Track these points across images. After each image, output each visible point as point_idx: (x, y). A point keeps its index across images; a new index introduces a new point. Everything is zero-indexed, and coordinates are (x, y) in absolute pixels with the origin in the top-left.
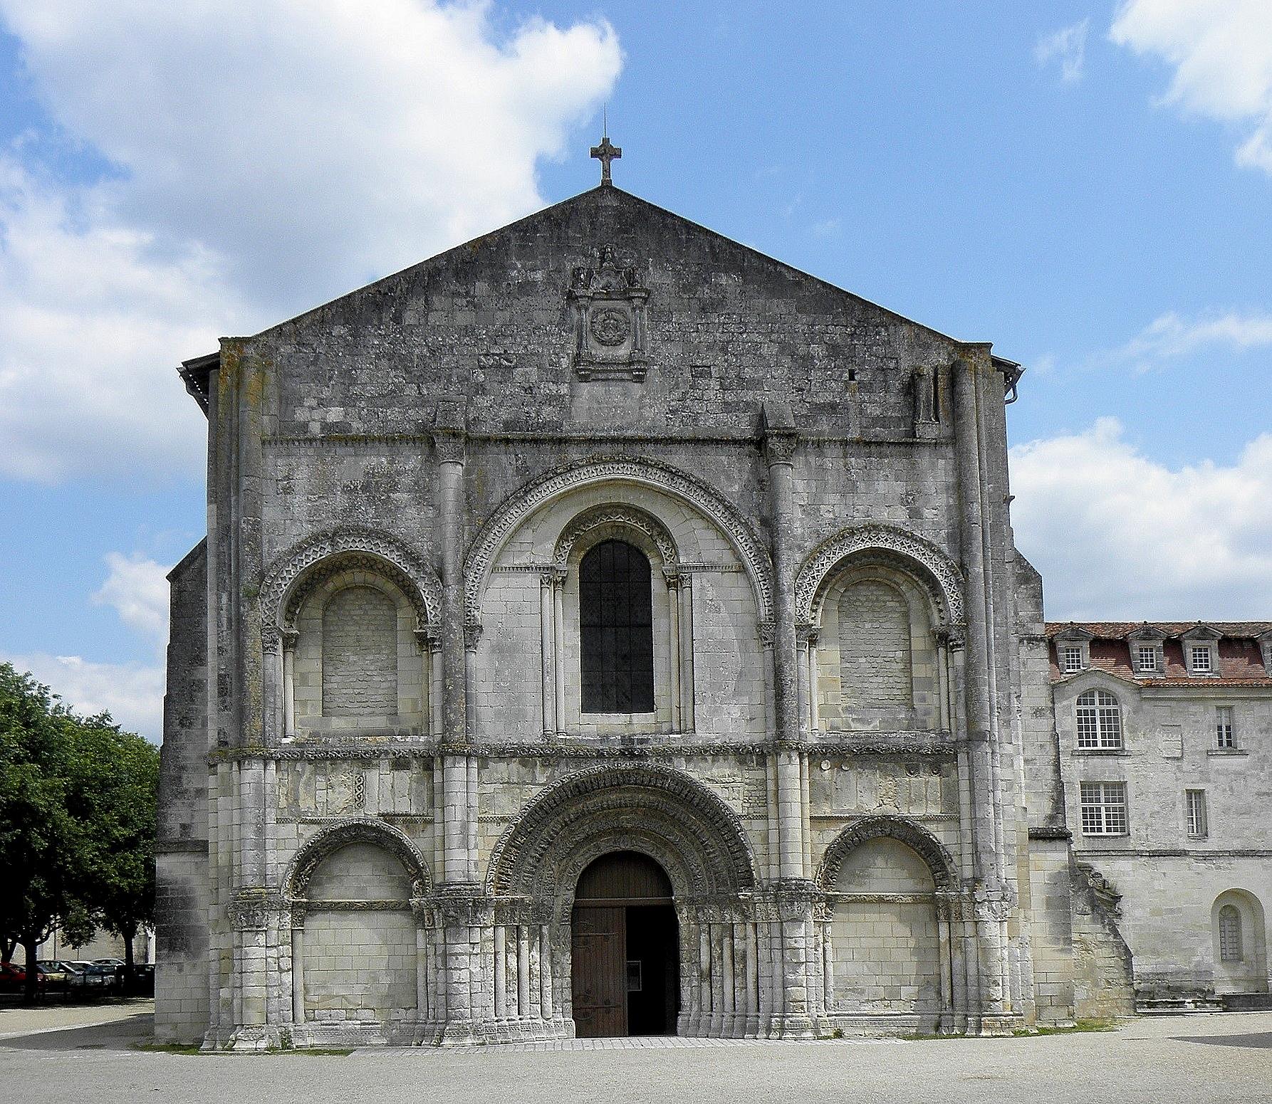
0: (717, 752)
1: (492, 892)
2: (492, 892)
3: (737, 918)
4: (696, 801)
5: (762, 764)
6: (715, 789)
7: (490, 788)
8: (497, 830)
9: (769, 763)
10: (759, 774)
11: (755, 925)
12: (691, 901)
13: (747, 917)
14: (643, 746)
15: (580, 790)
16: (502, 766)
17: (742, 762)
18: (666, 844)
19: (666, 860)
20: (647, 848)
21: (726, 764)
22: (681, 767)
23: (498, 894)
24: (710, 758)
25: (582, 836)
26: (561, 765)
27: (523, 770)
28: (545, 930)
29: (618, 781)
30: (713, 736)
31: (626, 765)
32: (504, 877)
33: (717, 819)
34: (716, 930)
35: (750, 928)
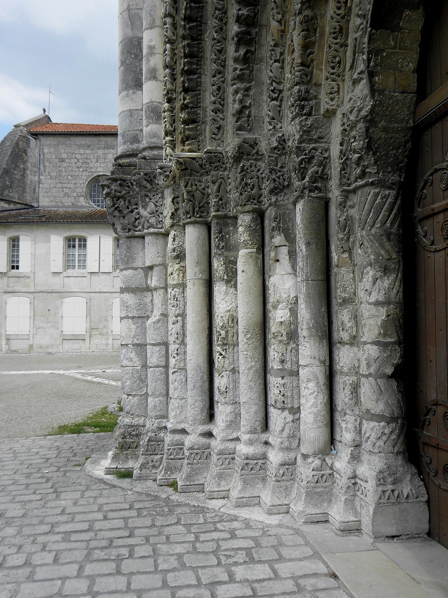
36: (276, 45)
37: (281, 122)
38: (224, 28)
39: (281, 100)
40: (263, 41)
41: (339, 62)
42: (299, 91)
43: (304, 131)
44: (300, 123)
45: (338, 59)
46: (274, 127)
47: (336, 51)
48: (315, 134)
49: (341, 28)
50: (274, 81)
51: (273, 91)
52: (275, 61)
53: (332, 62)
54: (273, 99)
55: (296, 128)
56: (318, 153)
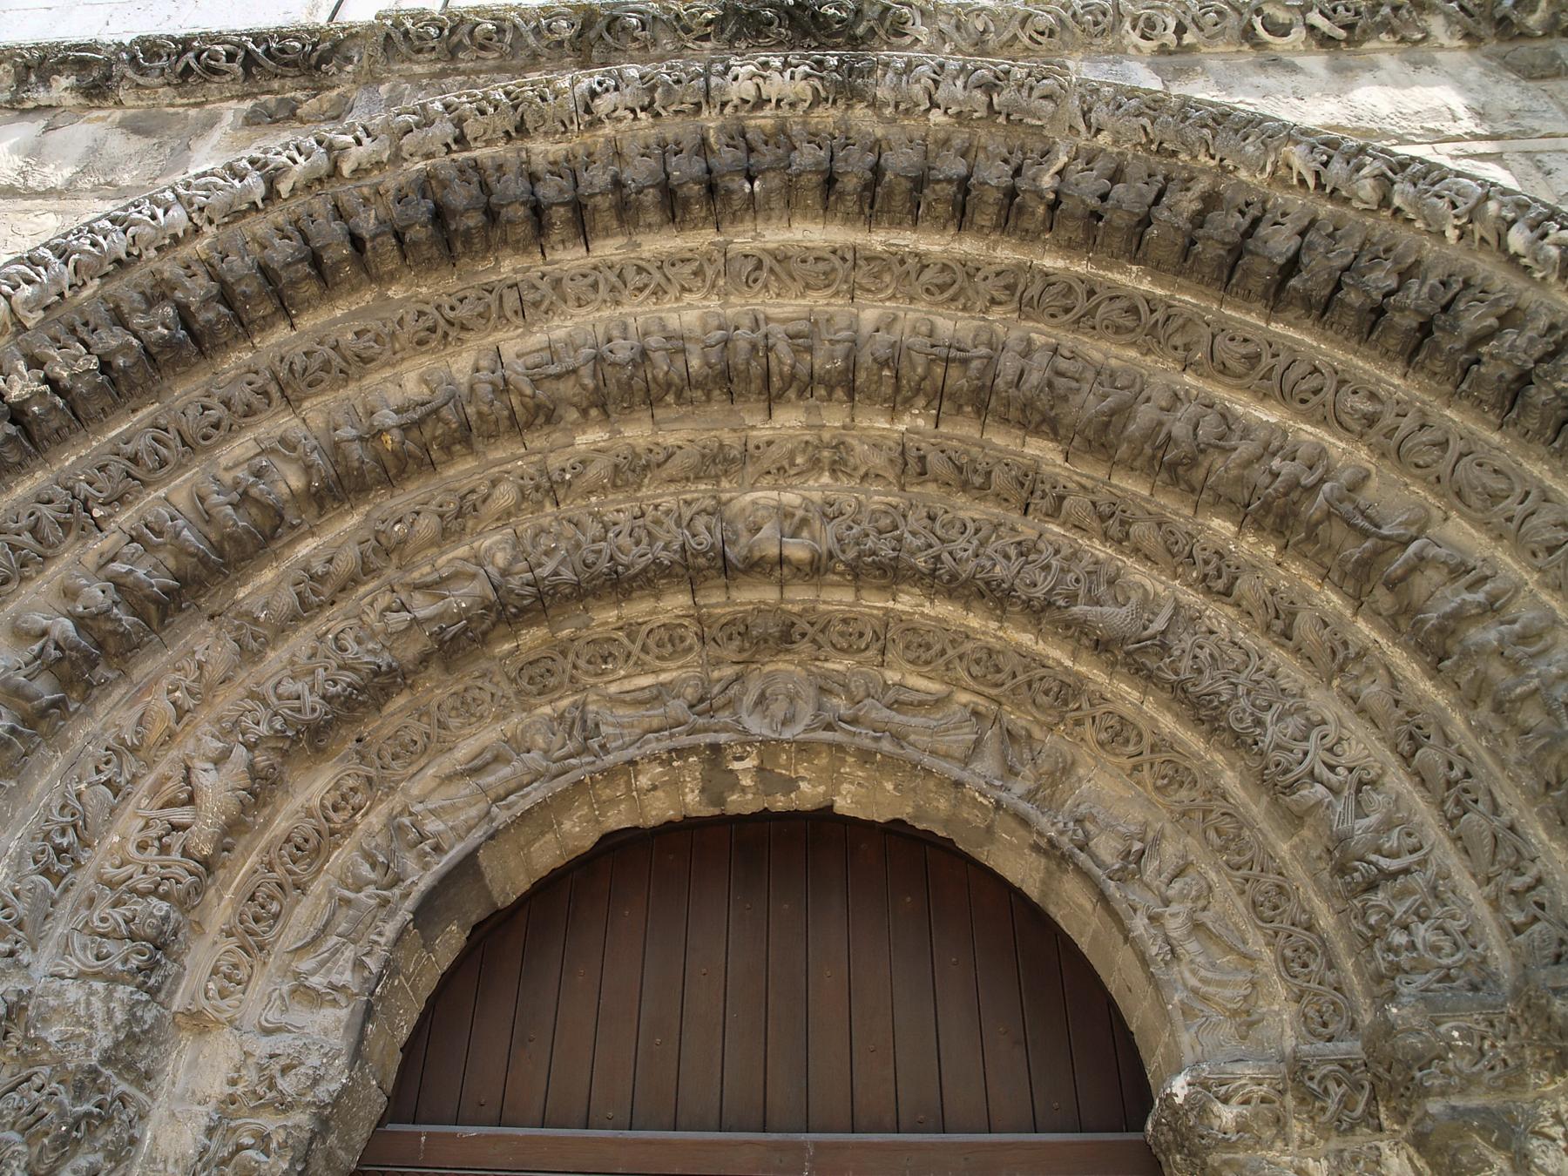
25: (461, 597)
36: (133, 750)
37: (34, 950)
38: (12, 586)
39: (66, 890)
40: (101, 709)
41: (276, 916)
42: (165, 919)
43: (131, 1036)
44: (132, 1007)
45: (275, 907)
46: (11, 954)
47: (280, 886)
48: (145, 1057)
49: (317, 850)
50: (75, 826)
51: (59, 851)
52: (107, 783)
53: (263, 907)
54: (46, 872)
55: (110, 1014)
56: (124, 1117)
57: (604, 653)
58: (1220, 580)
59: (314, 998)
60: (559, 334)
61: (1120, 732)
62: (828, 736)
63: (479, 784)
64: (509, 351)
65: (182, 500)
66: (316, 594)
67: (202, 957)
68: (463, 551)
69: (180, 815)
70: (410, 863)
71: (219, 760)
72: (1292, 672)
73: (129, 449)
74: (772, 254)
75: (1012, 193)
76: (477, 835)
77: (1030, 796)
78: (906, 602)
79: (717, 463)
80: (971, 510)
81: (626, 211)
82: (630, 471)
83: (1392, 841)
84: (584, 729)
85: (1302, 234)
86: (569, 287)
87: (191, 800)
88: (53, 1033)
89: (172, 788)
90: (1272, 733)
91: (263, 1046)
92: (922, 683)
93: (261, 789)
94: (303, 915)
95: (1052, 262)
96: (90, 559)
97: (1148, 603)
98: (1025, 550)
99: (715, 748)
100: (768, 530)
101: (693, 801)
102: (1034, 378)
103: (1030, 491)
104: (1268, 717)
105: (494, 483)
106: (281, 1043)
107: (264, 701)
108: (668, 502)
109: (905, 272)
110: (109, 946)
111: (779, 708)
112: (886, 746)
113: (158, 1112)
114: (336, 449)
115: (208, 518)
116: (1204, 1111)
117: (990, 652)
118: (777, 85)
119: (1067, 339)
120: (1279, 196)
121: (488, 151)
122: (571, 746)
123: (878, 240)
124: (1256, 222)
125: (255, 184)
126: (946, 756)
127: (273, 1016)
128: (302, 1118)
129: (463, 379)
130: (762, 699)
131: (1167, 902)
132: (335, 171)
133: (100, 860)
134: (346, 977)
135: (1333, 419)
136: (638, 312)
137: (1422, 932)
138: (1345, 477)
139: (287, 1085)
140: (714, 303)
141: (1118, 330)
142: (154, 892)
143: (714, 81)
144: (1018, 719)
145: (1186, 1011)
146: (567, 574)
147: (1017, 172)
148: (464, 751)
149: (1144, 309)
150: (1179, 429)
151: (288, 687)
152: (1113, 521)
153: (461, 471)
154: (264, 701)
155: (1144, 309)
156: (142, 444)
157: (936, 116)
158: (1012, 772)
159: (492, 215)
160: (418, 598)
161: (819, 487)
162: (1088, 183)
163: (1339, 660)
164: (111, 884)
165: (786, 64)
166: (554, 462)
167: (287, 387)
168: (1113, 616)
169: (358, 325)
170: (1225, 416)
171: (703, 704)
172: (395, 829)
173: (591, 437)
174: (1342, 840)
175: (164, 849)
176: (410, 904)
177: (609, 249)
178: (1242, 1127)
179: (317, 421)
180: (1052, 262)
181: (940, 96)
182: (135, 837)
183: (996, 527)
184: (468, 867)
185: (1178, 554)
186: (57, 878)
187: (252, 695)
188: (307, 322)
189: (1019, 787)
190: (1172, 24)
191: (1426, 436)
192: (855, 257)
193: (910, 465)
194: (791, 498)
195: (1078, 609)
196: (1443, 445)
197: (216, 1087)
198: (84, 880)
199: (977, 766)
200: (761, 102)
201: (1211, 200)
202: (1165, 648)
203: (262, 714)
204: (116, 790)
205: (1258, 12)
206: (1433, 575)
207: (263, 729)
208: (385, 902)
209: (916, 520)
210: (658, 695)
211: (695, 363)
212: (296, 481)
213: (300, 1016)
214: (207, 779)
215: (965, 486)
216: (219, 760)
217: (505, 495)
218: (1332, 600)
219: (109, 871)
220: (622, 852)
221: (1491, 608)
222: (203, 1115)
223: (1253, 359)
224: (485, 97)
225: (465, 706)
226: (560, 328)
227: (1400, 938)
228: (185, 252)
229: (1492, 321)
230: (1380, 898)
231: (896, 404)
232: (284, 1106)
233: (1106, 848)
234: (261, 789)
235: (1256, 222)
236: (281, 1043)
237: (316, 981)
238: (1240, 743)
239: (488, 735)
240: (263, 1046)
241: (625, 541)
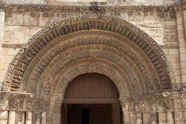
0: (147, 10)
1: (8, 90)
2: (8, 90)
3: (161, 109)
4: (135, 38)
5: (174, 17)
6: (147, 31)
7: (11, 28)
8: (14, 52)
9: (178, 15)
10: (171, 23)
11: (173, 113)
12: (131, 100)
13: (168, 108)
14: (103, 5)
15: (66, 31)
16: (20, 16)
17: (161, 16)
18: (116, 68)
19: (116, 76)
20: (104, 70)
21: (152, 17)
22: (125, 17)
23: (12, 90)
24: (142, 14)
25: (68, 61)
26: (54, 16)
27: (32, 19)
28: (44, 115)
29: (88, 26)
30: (144, 2)
31: (93, 16)
32: (16, 81)
33: (147, 48)
34: (146, 117)
35: (170, 115)
57: (79, 63)
58: (128, 61)
59: (59, 93)
60: (75, 39)
61: (119, 71)
62: (97, 70)
63: (68, 75)
64: (70, 40)
65: (45, 57)
66: (56, 61)
67: (51, 91)
68: (67, 57)
69: (49, 81)
70: (65, 81)
71: (51, 76)
72: (132, 70)
73: (41, 54)
74: (93, 31)
75: (114, 30)
76: (70, 79)
77: (112, 75)
78: (103, 59)
79: (88, 48)
80: (109, 52)
81: (81, 29)
82: (81, 49)
83: (136, 84)
84: (77, 69)
85: (137, 37)
86: (76, 36)
87: (49, 80)
88: (44, 99)
89: (47, 79)
90: (130, 75)
91: (57, 97)
92: (104, 65)
93: (54, 78)
94: (57, 86)
95: (117, 34)
96: (39, 63)
97: (122, 62)
98: (113, 57)
99: (88, 71)
100: (92, 54)
101: (86, 72)
102: (115, 45)
103: (114, 51)
104: (130, 73)
105: (70, 51)
106: (58, 96)
107: (53, 71)
108: (84, 51)
109: (105, 34)
110: (46, 92)
111: (93, 67)
112: (102, 71)
113: (51, 102)
114: (57, 51)
115: (48, 58)
116: (121, 100)
117: (110, 64)
118: (94, 18)
119: (118, 40)
120: (136, 33)
121: (68, 24)
122: (76, 71)
123: (102, 31)
124: (133, 35)
125: (48, 29)
126: (106, 72)
127: (57, 94)
128: (61, 102)
129: (67, 43)
130: (92, 66)
131: (121, 84)
132: (55, 26)
133: (44, 86)
134: (62, 91)
135: (137, 52)
136: (81, 37)
137: (136, 91)
138: (137, 57)
139: (59, 99)
140: (88, 36)
141: (122, 41)
142: (48, 88)
143: (89, 17)
144: (112, 69)
145: (122, 93)
146: (76, 59)
147: (115, 28)
148: (68, 71)
149: (124, 39)
150: (126, 51)
151: (55, 70)
152: (120, 55)
153: (67, 51)
154: (53, 71)
155: (124, 39)
156: (42, 53)
157: (108, 21)
158: (111, 73)
159: (69, 31)
160: (64, 61)
161: (96, 50)
162: (121, 29)
163: (135, 70)
164: (45, 87)
165: (95, 16)
166: (75, 49)
167: (52, 46)
168: (119, 63)
169: (58, 40)
170: (130, 49)
171: (87, 66)
172: (63, 78)
173: (77, 47)
174: (133, 84)
175: (48, 84)
176: (65, 85)
177: (79, 31)
178: (124, 101)
179: (55, 48)
180: (117, 34)
181: (109, 19)
182: (46, 83)
183: (111, 54)
184: (69, 81)
185: (125, 59)
186: (42, 88)
187: (52, 70)
188: (53, 40)
189: (112, 74)
190: (130, 9)
191: (143, 56)
192: (100, 32)
193: (104, 49)
194: (94, 51)
195: (117, 62)
196: (144, 57)
197: (55, 100)
198: (43, 87)
199: (109, 72)
200: (93, 19)
201: (130, 33)
202: (123, 67)
203: (53, 72)
204: (44, 80)
205: (138, 8)
206: (141, 66)
207: (53, 74)
208: (63, 85)
209: (105, 53)
210: (83, 65)
211: (87, 42)
212: (54, 54)
213: (59, 94)
214: (50, 78)
215: (109, 51)
216: (51, 76)
217: (71, 52)
218: (135, 65)
219: (45, 86)
220: (79, 76)
221: (145, 70)
222: (54, 102)
223: (132, 46)
224: (68, 19)
225: (68, 68)
226: (75, 38)
227: (135, 91)
228: (43, 36)
229: (148, 49)
230: (134, 88)
231: (104, 44)
232: (59, 101)
233: (118, 80)
234: (54, 78)
235: (133, 35)
236: (58, 96)
237: (59, 91)
238: (128, 75)
239: (70, 70)
240: (57, 97)
241: (80, 55)
